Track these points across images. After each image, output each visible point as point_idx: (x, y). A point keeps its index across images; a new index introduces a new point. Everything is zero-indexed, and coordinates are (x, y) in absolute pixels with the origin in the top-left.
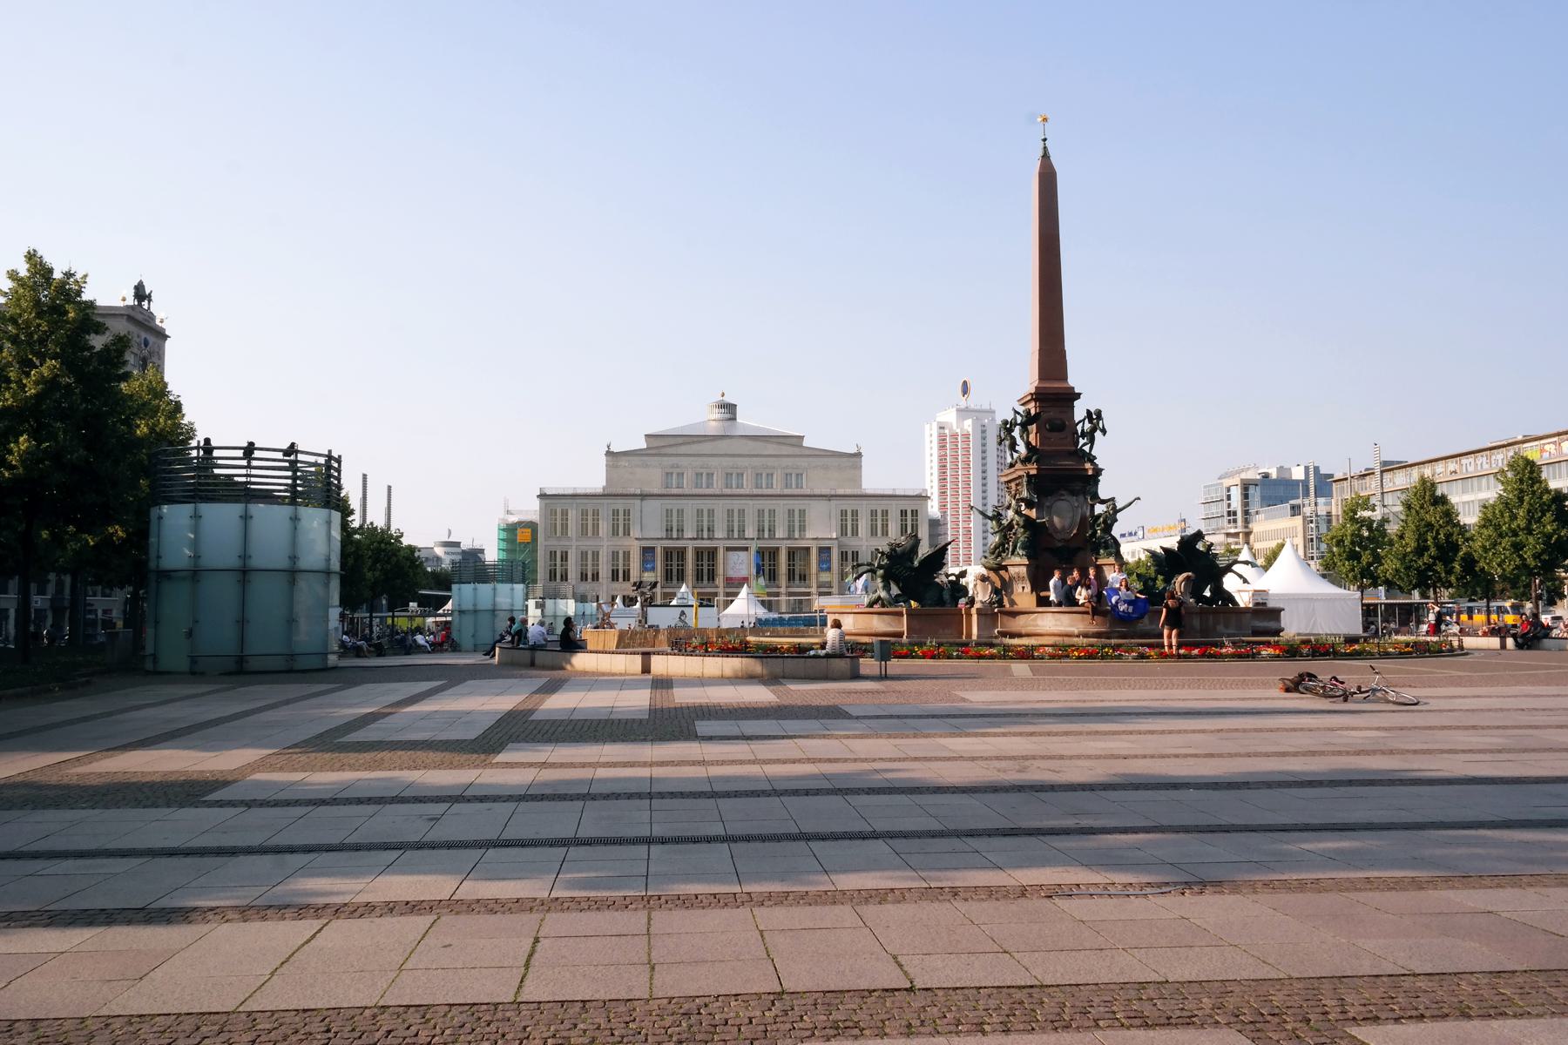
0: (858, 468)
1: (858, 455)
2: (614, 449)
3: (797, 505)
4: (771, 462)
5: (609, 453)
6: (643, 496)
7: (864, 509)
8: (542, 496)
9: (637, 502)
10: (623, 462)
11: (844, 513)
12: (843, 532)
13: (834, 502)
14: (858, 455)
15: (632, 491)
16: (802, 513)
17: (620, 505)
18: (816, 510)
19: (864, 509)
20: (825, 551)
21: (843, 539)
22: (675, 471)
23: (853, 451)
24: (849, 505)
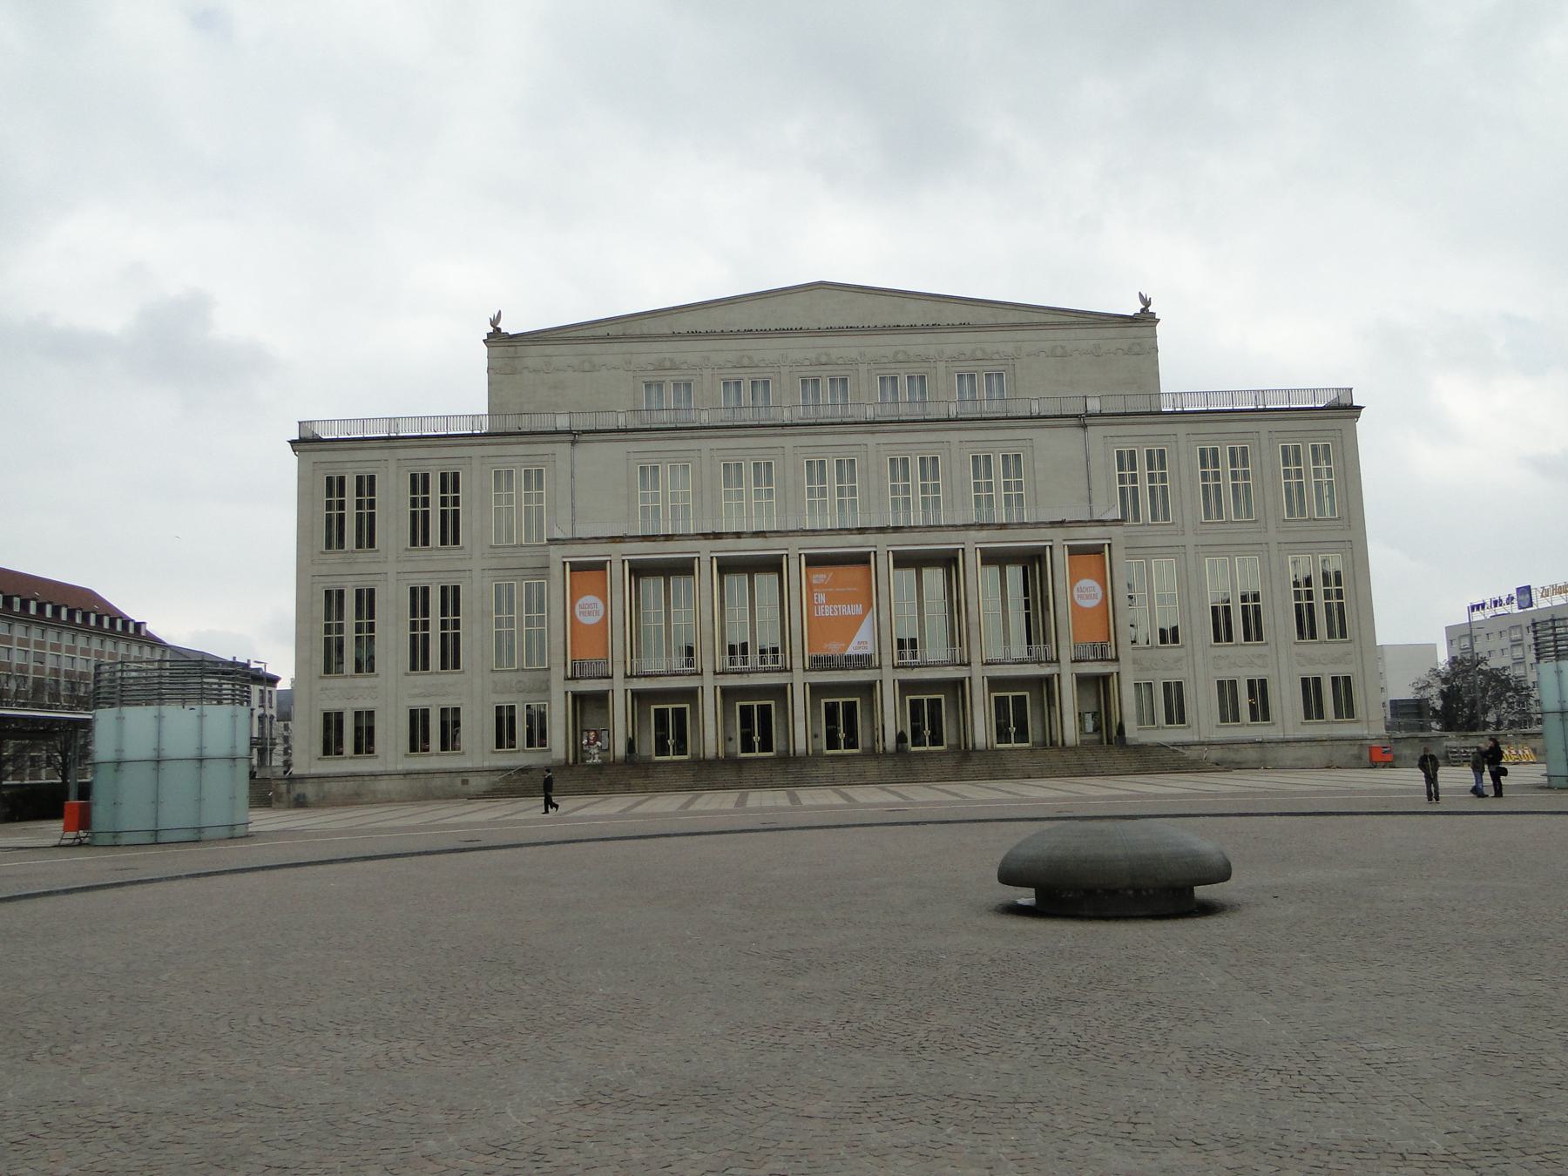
0: (1150, 351)
1: (1146, 319)
2: (507, 327)
3: (997, 442)
4: (917, 344)
5: (496, 338)
6: (574, 436)
7: (1183, 452)
9: (563, 449)
10: (533, 353)
11: (1126, 460)
13: (1095, 433)
16: (1013, 462)
17: (516, 455)
19: (1183, 452)
22: (669, 378)
23: (1134, 308)
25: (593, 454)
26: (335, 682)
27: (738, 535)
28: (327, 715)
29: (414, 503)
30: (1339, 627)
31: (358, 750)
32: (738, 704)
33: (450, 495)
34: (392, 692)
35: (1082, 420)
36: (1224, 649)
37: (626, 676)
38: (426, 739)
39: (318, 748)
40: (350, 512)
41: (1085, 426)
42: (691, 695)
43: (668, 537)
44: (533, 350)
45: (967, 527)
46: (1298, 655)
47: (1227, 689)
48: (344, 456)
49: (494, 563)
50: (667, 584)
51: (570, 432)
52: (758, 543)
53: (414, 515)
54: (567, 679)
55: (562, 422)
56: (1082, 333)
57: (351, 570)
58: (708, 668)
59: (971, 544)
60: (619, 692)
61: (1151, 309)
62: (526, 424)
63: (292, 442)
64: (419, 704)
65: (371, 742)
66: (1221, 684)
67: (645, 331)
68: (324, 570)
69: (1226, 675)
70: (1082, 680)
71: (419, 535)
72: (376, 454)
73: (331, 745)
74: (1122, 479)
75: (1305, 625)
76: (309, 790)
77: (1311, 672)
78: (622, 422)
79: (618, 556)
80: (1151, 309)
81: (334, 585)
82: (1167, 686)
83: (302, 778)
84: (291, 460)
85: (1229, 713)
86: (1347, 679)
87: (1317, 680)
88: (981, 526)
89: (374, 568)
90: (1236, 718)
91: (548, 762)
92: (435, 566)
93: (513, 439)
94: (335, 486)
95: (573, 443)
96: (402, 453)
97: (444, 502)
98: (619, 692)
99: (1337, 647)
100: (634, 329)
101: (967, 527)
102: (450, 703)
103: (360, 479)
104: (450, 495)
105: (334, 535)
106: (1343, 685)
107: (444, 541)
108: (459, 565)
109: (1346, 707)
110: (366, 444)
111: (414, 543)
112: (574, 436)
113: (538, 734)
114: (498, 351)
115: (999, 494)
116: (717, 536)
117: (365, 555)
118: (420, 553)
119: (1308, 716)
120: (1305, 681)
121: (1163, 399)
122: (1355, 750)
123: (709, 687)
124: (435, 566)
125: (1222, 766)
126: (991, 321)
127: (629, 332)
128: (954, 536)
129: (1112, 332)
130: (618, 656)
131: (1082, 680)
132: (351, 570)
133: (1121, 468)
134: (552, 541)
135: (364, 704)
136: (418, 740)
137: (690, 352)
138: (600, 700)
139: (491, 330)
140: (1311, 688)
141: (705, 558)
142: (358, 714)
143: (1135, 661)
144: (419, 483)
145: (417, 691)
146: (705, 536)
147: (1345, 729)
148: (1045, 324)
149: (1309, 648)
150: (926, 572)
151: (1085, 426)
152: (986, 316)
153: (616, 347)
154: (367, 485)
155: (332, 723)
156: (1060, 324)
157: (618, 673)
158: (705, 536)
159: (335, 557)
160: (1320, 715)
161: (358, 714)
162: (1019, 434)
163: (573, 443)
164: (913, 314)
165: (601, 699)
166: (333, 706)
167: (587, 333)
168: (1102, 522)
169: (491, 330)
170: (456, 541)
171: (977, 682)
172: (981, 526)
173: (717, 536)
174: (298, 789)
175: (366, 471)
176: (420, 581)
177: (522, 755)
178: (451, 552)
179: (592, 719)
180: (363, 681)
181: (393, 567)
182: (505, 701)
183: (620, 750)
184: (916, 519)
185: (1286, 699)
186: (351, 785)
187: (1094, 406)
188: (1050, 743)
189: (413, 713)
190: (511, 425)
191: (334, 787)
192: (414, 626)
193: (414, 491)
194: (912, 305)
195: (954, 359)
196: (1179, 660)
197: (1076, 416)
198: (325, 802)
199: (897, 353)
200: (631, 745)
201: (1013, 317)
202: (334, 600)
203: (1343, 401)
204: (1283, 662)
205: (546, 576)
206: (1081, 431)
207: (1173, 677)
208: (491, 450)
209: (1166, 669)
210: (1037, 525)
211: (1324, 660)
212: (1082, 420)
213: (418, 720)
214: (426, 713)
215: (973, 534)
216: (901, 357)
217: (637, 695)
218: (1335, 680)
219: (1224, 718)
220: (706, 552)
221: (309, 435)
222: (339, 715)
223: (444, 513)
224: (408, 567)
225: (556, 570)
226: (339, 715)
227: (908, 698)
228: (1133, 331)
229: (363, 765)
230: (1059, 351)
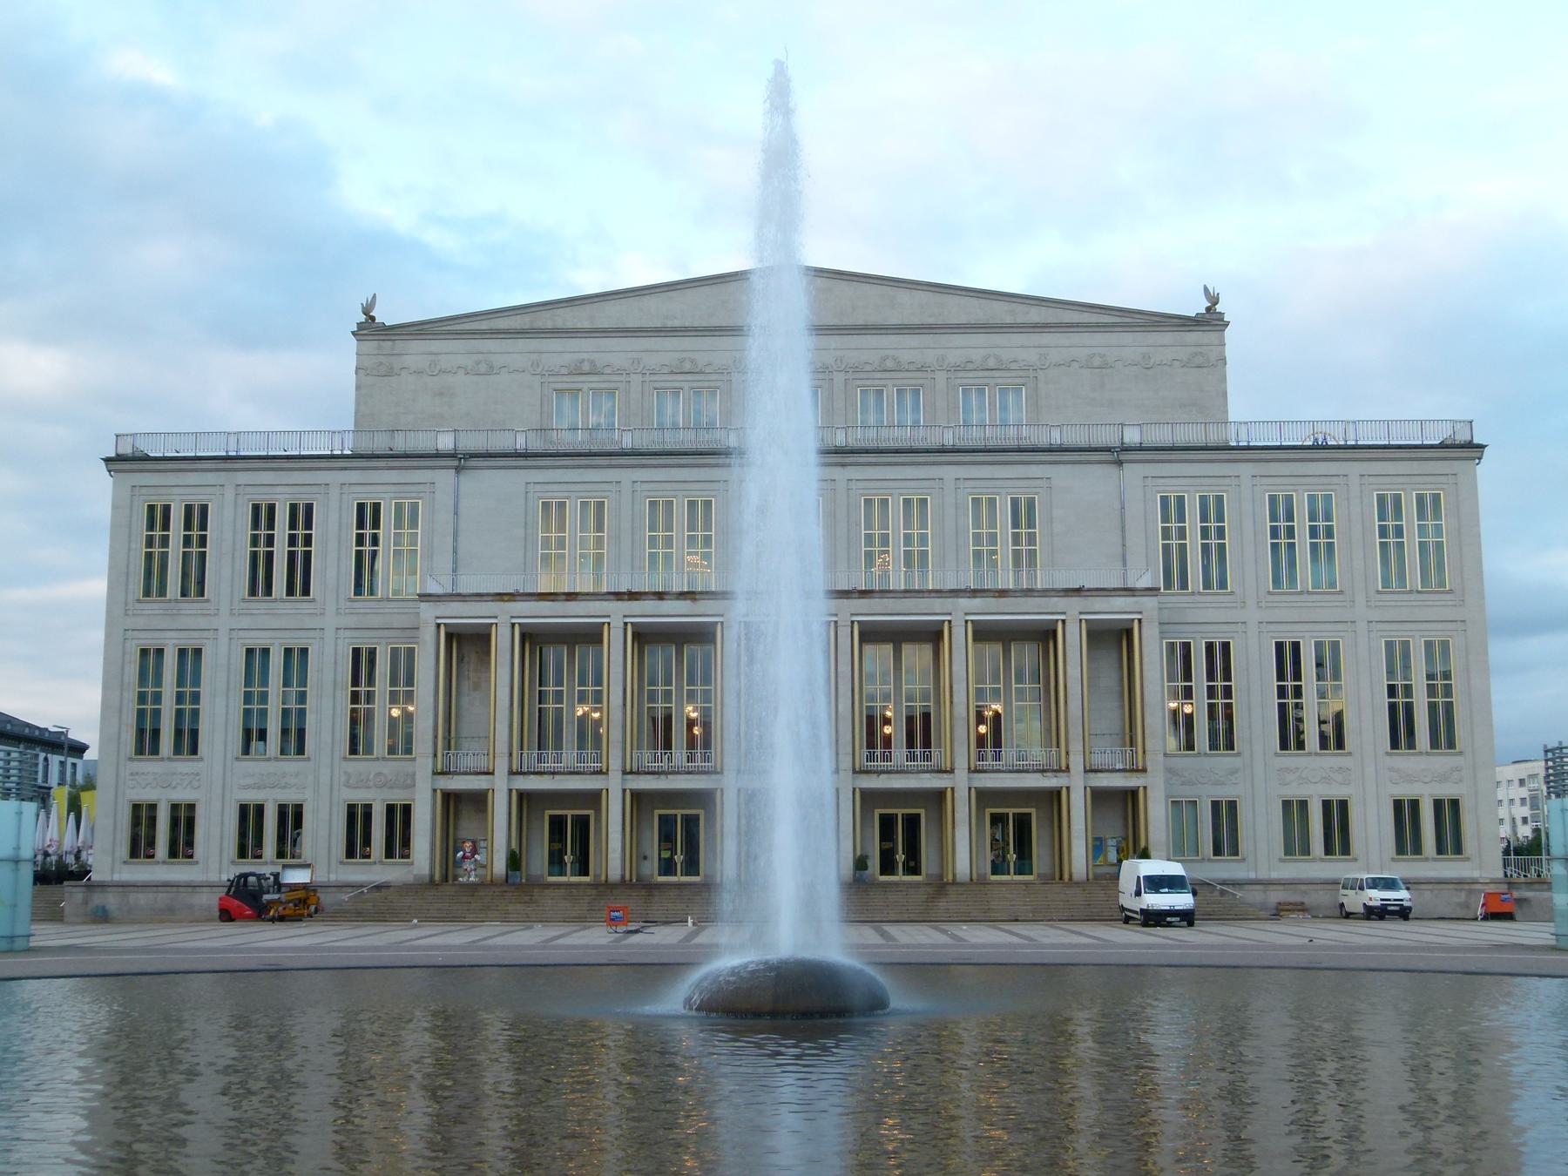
1: (1211, 320)
2: (386, 315)
4: (909, 349)
5: (369, 329)
6: (461, 460)
7: (1247, 501)
8: (115, 462)
9: (444, 478)
10: (415, 352)
11: (1173, 509)
12: (1175, 575)
14: (1211, 320)
15: (421, 443)
18: (1077, 490)
20: (1113, 640)
21: (1175, 598)
23: (1197, 306)
24: (1190, 482)
25: (486, 484)
26: (149, 766)
27: (660, 596)
28: (136, 807)
29: (255, 541)
30: (1444, 735)
31: (173, 853)
32: (657, 812)
33: (300, 532)
34: (218, 782)
35: (1118, 455)
36: (1293, 759)
37: (511, 773)
38: (259, 843)
39: (124, 850)
40: (175, 550)
41: (1120, 463)
42: (594, 799)
43: (571, 596)
44: (415, 346)
45: (955, 593)
46: (1391, 769)
47: (1295, 810)
48: (171, 479)
49: (352, 621)
50: (571, 655)
51: (453, 455)
52: (683, 606)
53: (254, 556)
54: (435, 773)
55: (445, 443)
56: (1127, 337)
57: (174, 623)
58: (615, 764)
59: (960, 615)
60: (501, 790)
61: (1219, 308)
62: (401, 444)
63: (107, 460)
64: (252, 797)
65: (190, 843)
66: (1287, 804)
67: (559, 324)
68: (140, 622)
69: (1295, 792)
70: (1100, 798)
71: (260, 583)
72: (211, 478)
73: (140, 846)
74: (1166, 533)
75: (1400, 732)
76: (111, 900)
77: (1406, 791)
78: (521, 444)
79: (504, 622)
80: (1219, 308)
81: (151, 641)
82: (1216, 805)
83: (103, 886)
84: (103, 484)
85: (1296, 844)
86: (1455, 804)
87: (1415, 804)
88: (974, 593)
89: (202, 623)
90: (1306, 850)
91: (410, 879)
92: (276, 622)
93: (382, 463)
94: (158, 517)
95: (458, 469)
96: (243, 478)
97: (292, 540)
98: (501, 790)
99: (1442, 761)
100: (546, 320)
101: (955, 593)
102: (290, 797)
103: (189, 509)
104: (300, 532)
105: (153, 581)
106: (1449, 812)
107: (290, 591)
108: (308, 623)
109: (1451, 840)
110: (198, 465)
111: (253, 592)
112: (461, 460)
113: (399, 843)
114: (370, 346)
115: (1005, 549)
116: (633, 596)
117: (191, 607)
118: (260, 605)
119: (1400, 849)
120: (1398, 804)
121: (1233, 428)
122: (1463, 896)
123: (614, 788)
124: (276, 622)
125: (1279, 912)
126: (1008, 320)
127: (539, 324)
128: (937, 604)
129: (1167, 337)
130: (502, 747)
131: (1100, 798)
132: (174, 623)
133: (1165, 519)
134: (425, 597)
135: (183, 795)
136: (248, 845)
137: (616, 352)
138: (478, 801)
139: (363, 318)
140: (1405, 812)
141: (617, 623)
142: (175, 807)
143: (1170, 771)
144: (263, 516)
145: (249, 781)
146: (618, 596)
147: (1450, 869)
148: (1078, 325)
149: (1405, 761)
150: (907, 649)
151: (1120, 463)
152: (1002, 313)
153: (522, 344)
154: (197, 517)
155: (142, 816)
156: (1098, 325)
157: (501, 767)
158: (618, 596)
159: (154, 607)
160: (1417, 849)
161: (175, 807)
162: (1034, 471)
163: (458, 469)
164: (909, 309)
165: (478, 801)
166: (146, 795)
167: (484, 325)
168: (1130, 591)
169: (363, 318)
170: (306, 591)
171: (962, 795)
172: (974, 593)
173: (633, 596)
174: (98, 899)
175: (197, 499)
176: (258, 640)
177: (378, 868)
178: (298, 605)
179: (468, 827)
180: (185, 766)
181: (226, 622)
182: (359, 796)
183: (500, 866)
184: (897, 582)
185: (1372, 827)
186: (163, 898)
187: (1132, 436)
188: (1058, 874)
189: (244, 809)
190: (380, 444)
191: (142, 899)
192: (248, 698)
193: (256, 525)
194: (904, 296)
195: (957, 368)
196: (1234, 772)
197: (1108, 449)
198: (132, 918)
199: (884, 359)
200: (514, 861)
201: (1036, 315)
202: (150, 658)
203: (1462, 437)
204: (1371, 779)
205: (415, 639)
206: (1113, 469)
207: (1224, 794)
208: (354, 476)
209: (1216, 783)
210: (1046, 593)
211: (1424, 775)
212: (1118, 455)
213: (249, 817)
214: (260, 809)
215: (964, 603)
216: (889, 364)
217: (522, 795)
218: (1438, 804)
219: (1289, 850)
220: (617, 616)
221: (126, 450)
222: (153, 807)
223: (292, 555)
224: (245, 622)
225: (428, 634)
226: (153, 807)
227: (877, 812)
228: (1192, 337)
229: (179, 872)
230: (1097, 361)
